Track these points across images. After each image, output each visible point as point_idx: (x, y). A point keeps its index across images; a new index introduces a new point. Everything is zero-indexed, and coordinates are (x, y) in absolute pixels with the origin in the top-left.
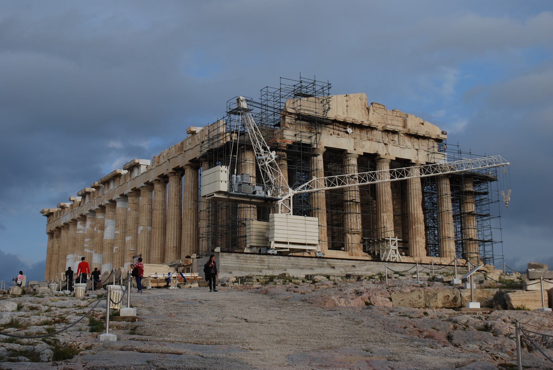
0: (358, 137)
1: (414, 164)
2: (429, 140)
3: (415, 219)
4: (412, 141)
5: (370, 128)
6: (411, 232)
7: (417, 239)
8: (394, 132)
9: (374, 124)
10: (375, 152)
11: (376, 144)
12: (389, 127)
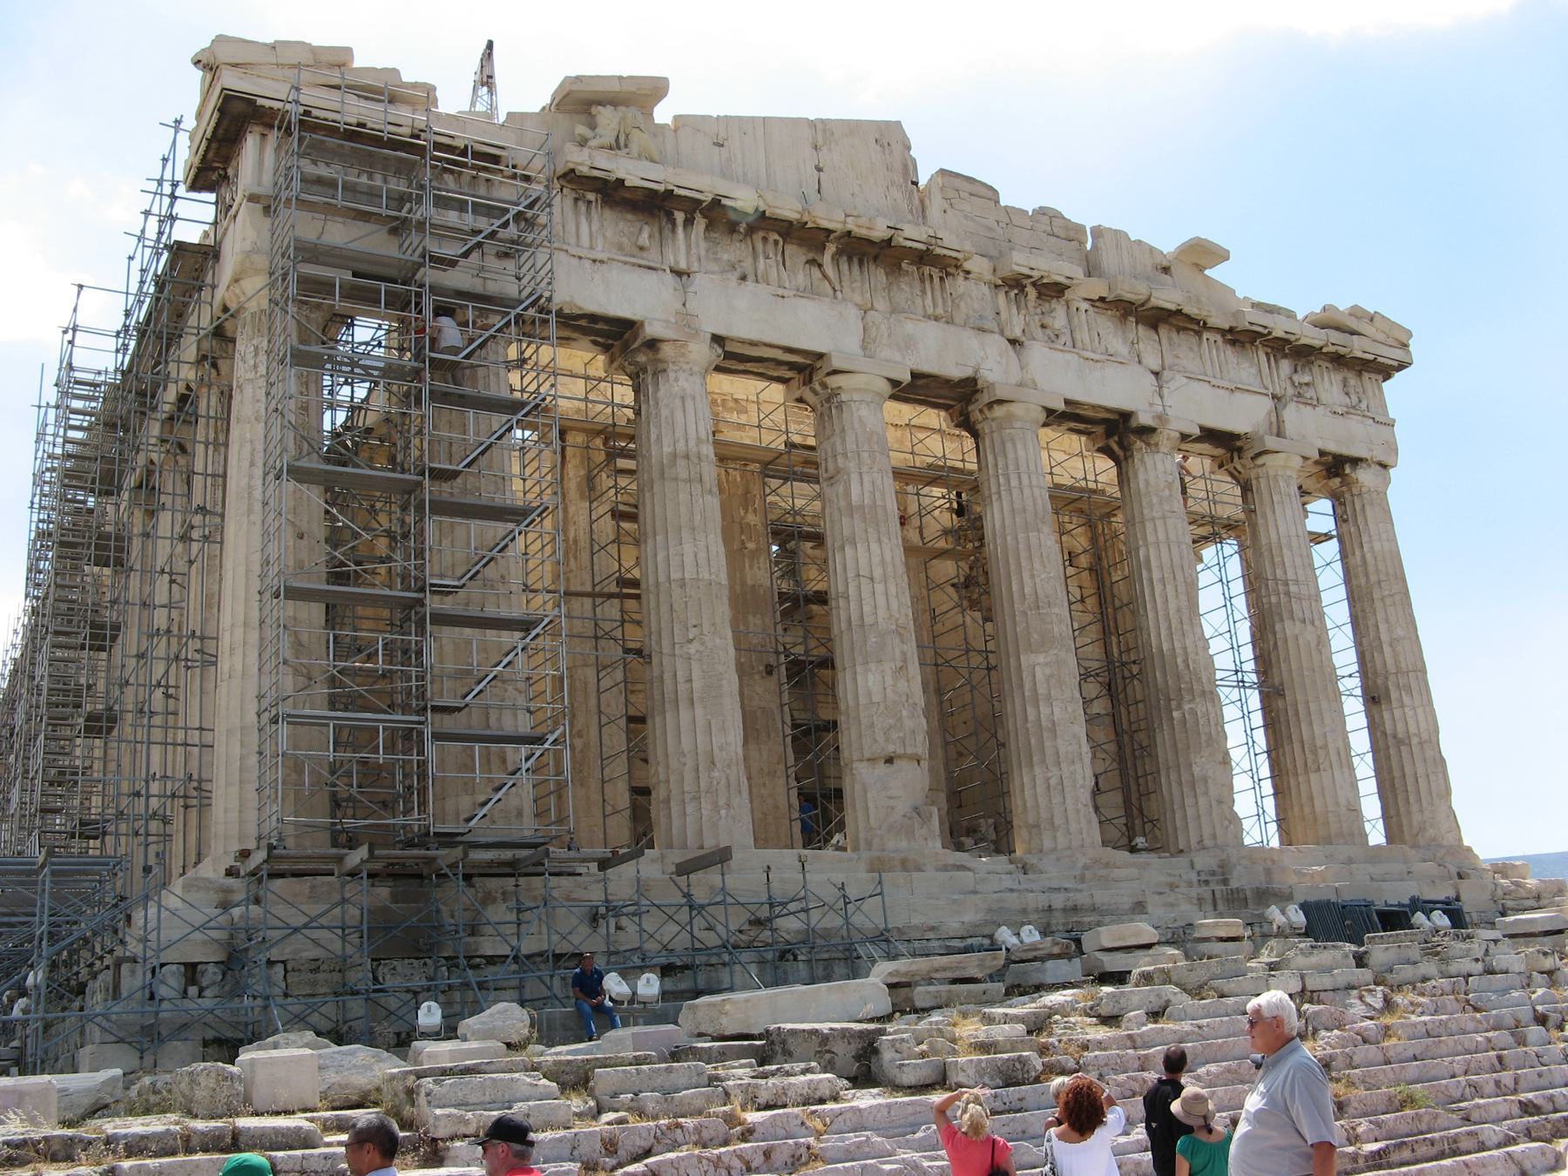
0: (881, 304)
2: (1198, 334)
3: (1178, 677)
4: (1131, 336)
5: (932, 263)
6: (1163, 739)
7: (1196, 770)
9: (951, 240)
10: (969, 372)
11: (971, 341)
12: (1021, 262)
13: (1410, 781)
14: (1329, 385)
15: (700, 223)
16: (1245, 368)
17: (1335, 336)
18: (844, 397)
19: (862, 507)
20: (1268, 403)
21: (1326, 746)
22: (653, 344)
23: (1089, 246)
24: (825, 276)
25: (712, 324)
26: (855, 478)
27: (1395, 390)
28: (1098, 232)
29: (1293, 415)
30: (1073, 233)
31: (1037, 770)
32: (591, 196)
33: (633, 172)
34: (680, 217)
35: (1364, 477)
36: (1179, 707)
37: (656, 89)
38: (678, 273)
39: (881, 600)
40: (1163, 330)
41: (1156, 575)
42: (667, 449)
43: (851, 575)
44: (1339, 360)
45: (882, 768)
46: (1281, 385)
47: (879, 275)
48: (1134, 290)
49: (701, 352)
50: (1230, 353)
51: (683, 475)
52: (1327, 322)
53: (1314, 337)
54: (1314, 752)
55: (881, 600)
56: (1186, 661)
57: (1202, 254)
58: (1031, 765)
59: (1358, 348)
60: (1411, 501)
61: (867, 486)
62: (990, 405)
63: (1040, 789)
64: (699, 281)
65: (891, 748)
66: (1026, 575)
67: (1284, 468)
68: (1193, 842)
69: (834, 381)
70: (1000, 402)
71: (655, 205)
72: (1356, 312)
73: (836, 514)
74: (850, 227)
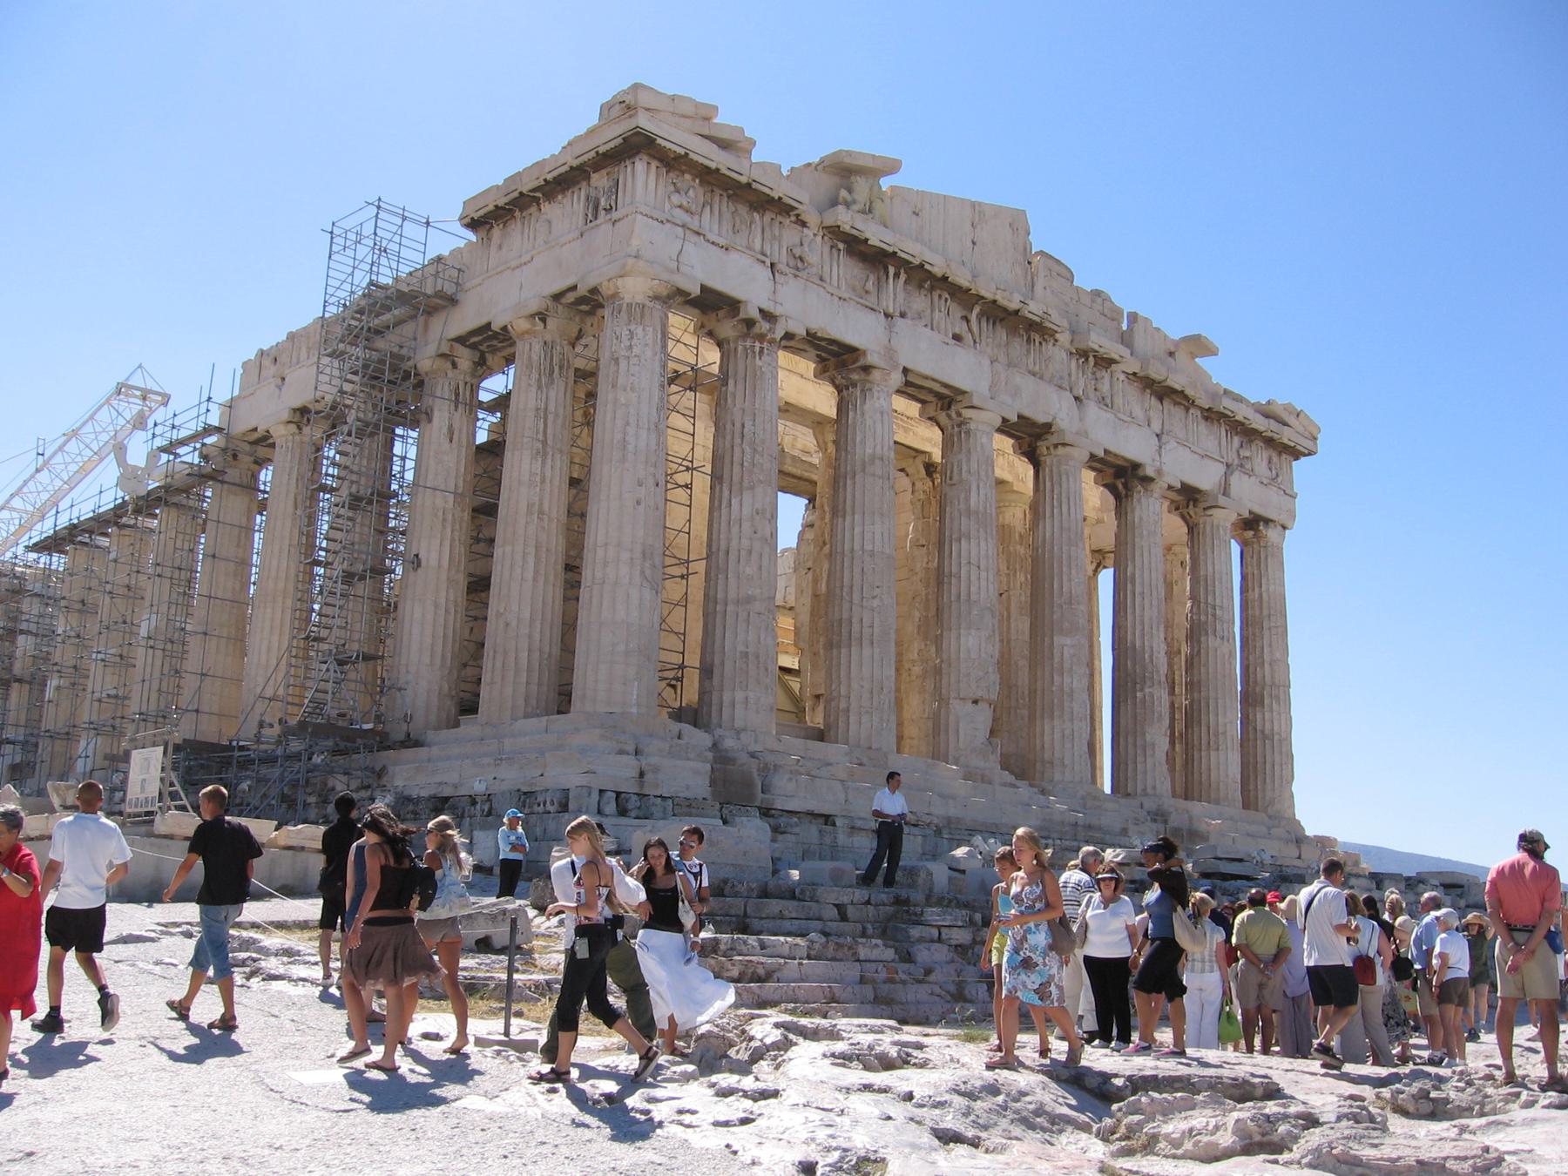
0: (1002, 358)
1: (1147, 480)
5: (1035, 330)
7: (1148, 737)
8: (1105, 362)
9: (1056, 319)
13: (1268, 766)
14: (1260, 458)
15: (903, 277)
16: (1210, 438)
17: (1274, 425)
18: (972, 426)
19: (977, 513)
20: (1222, 469)
21: (1224, 733)
22: (867, 369)
23: (1125, 327)
24: (970, 330)
26: (974, 488)
27: (1300, 466)
28: (1133, 317)
29: (1238, 482)
30: (1114, 314)
31: (1056, 722)
32: (841, 246)
33: (876, 235)
34: (892, 270)
35: (1271, 534)
36: (1142, 690)
37: (892, 167)
38: (887, 315)
39: (983, 583)
40: (1166, 402)
41: (1138, 589)
42: (869, 451)
43: (964, 562)
44: (1270, 442)
45: (969, 706)
46: (1232, 458)
47: (1002, 334)
48: (1156, 372)
49: (897, 379)
50: (1203, 427)
51: (879, 472)
53: (1259, 423)
54: (1217, 735)
55: (983, 583)
56: (1151, 657)
57: (1198, 345)
58: (1052, 718)
59: (1286, 436)
60: (1299, 555)
61: (982, 497)
62: (1056, 446)
63: (1057, 736)
65: (979, 694)
66: (1065, 578)
67: (1224, 518)
68: (1140, 788)
69: (967, 413)
70: (1064, 445)
72: (1289, 408)
73: (956, 514)
74: (998, 297)
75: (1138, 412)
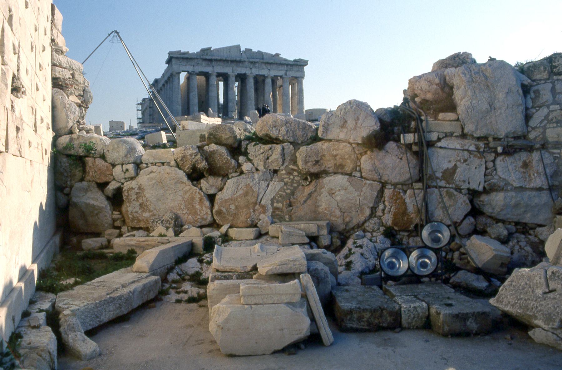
1: (267, 77)
25: (216, 71)
33: (208, 57)
35: (300, 79)
44: (297, 65)
52: (295, 61)
57: (277, 55)
59: (299, 63)
64: (215, 67)
71: (211, 60)
72: (300, 59)
75: (265, 67)
